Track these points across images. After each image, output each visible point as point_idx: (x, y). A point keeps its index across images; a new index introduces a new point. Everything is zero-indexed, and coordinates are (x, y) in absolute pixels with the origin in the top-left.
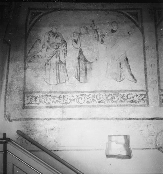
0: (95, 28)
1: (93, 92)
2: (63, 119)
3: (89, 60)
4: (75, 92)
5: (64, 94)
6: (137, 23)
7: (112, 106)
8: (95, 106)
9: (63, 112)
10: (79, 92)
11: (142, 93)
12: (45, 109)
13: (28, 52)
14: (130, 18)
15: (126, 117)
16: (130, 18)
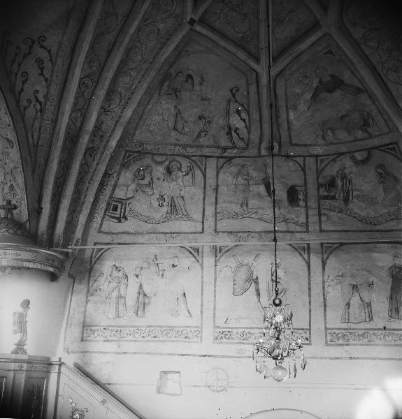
0: (157, 262)
1: (149, 327)
2: (118, 353)
3: (148, 295)
4: (132, 327)
5: (122, 329)
6: (198, 258)
7: (166, 341)
8: (149, 341)
9: (119, 346)
10: (135, 327)
11: (196, 329)
12: (101, 343)
13: (91, 285)
14: (191, 253)
15: (179, 353)
16: (191, 253)
